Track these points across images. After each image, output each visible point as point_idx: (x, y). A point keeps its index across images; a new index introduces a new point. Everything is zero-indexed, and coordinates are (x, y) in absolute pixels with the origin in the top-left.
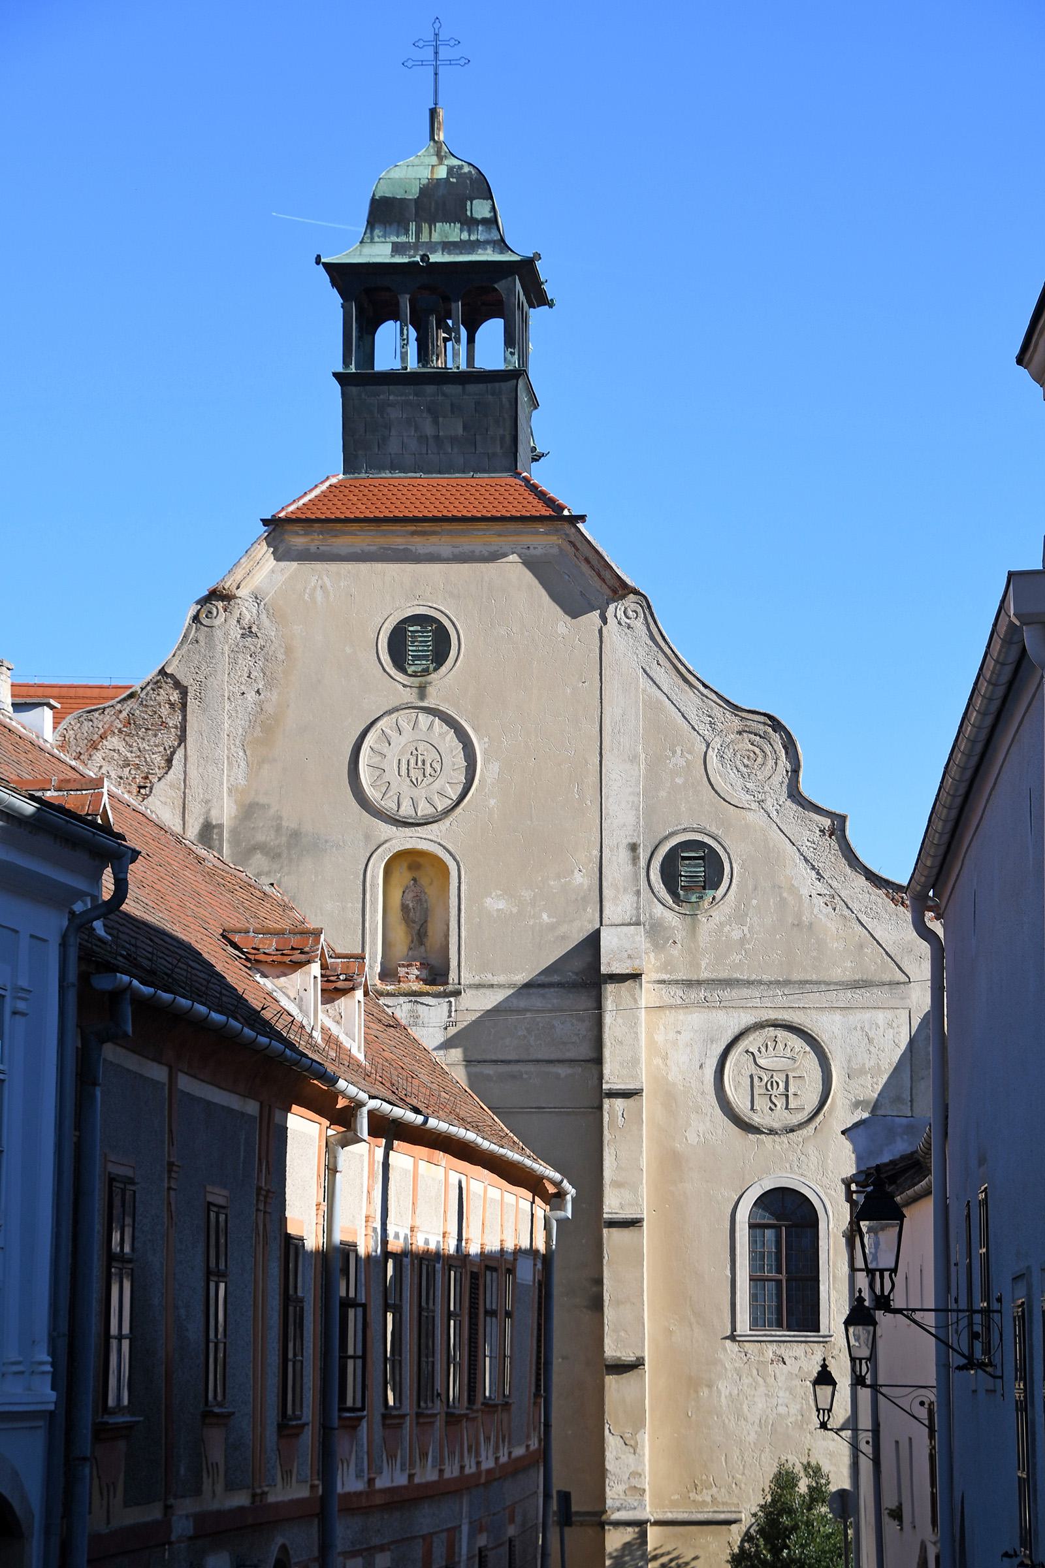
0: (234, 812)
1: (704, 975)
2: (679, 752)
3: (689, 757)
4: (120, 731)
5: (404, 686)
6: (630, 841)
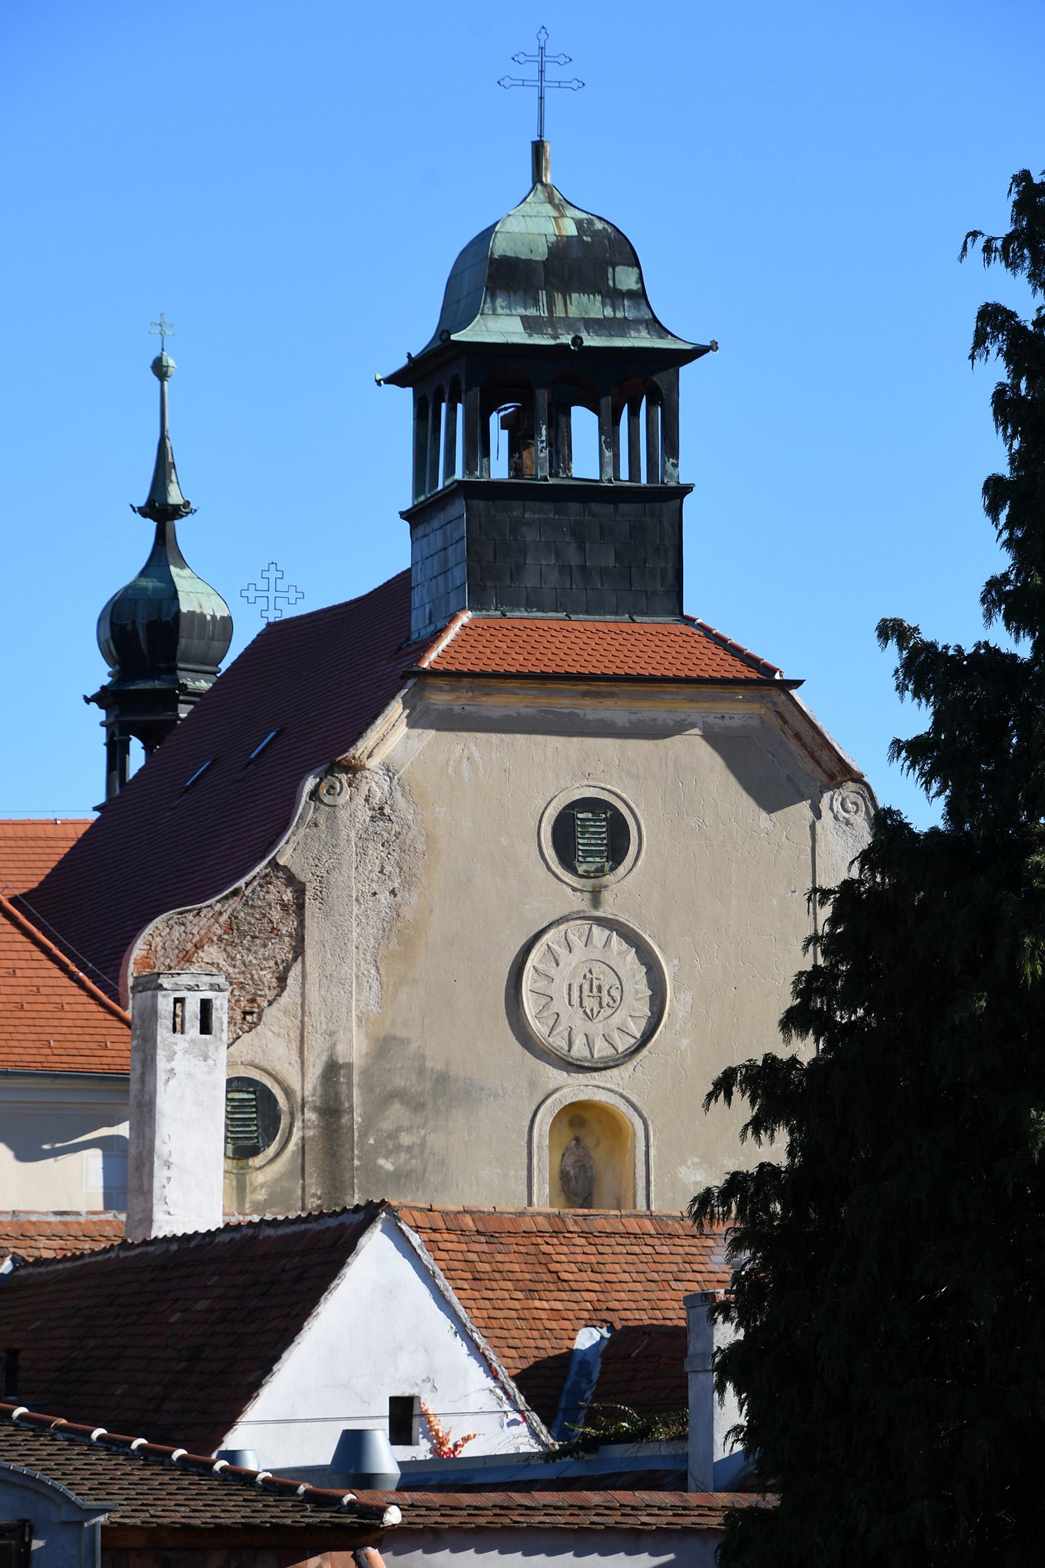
0: (365, 1048)
4: (220, 939)
5: (574, 889)
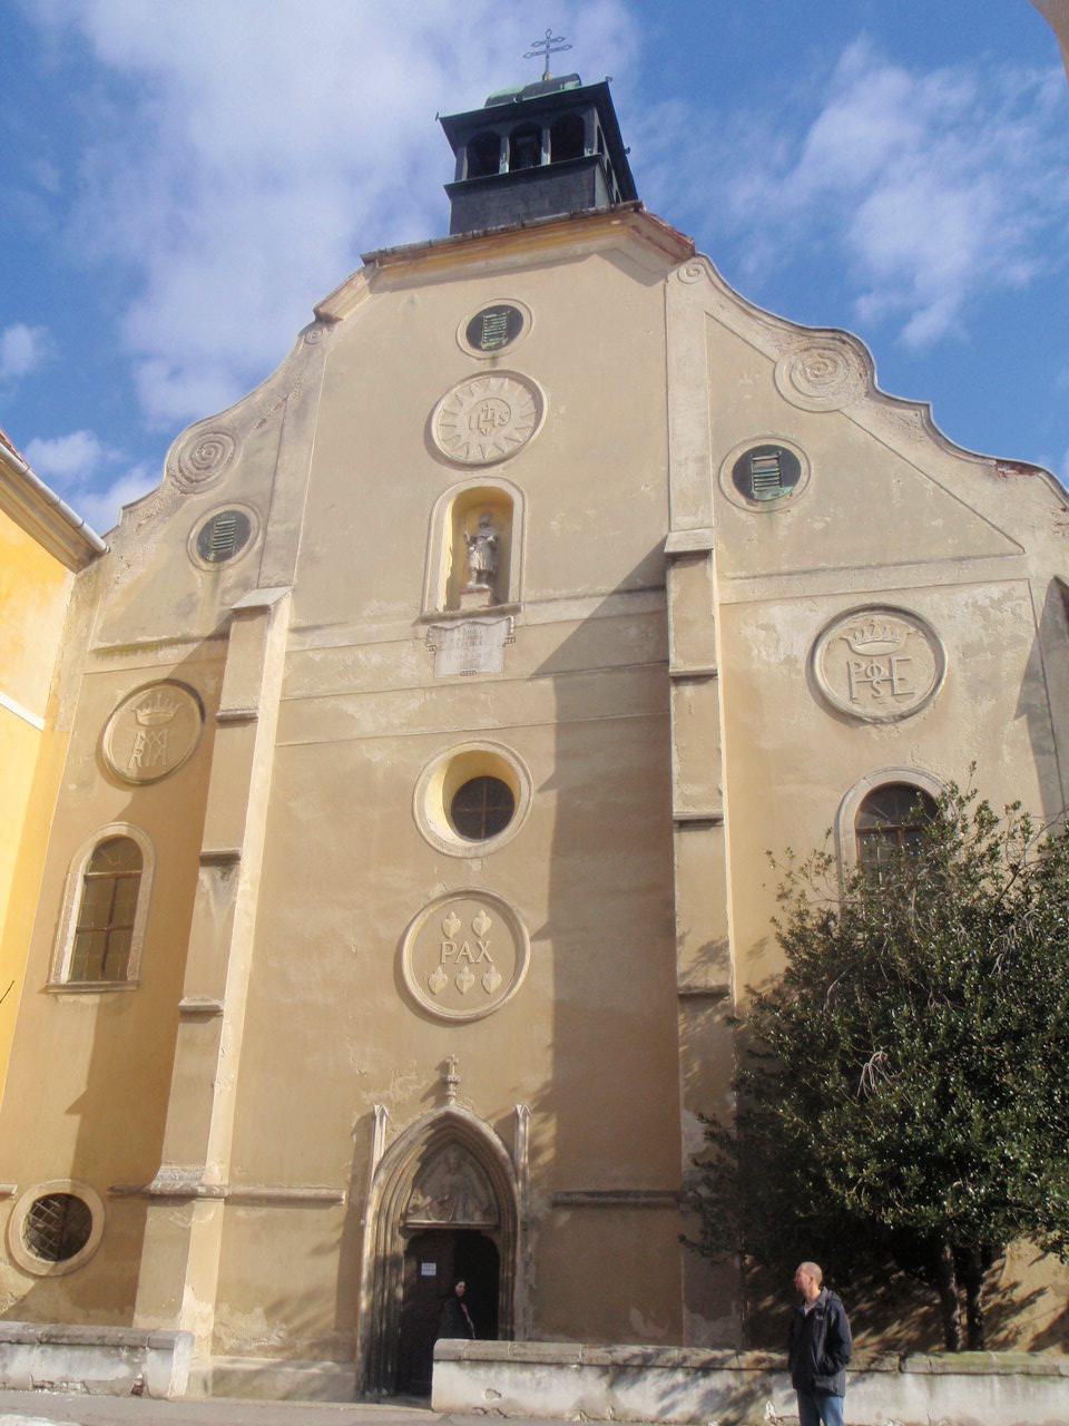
5: (479, 359)
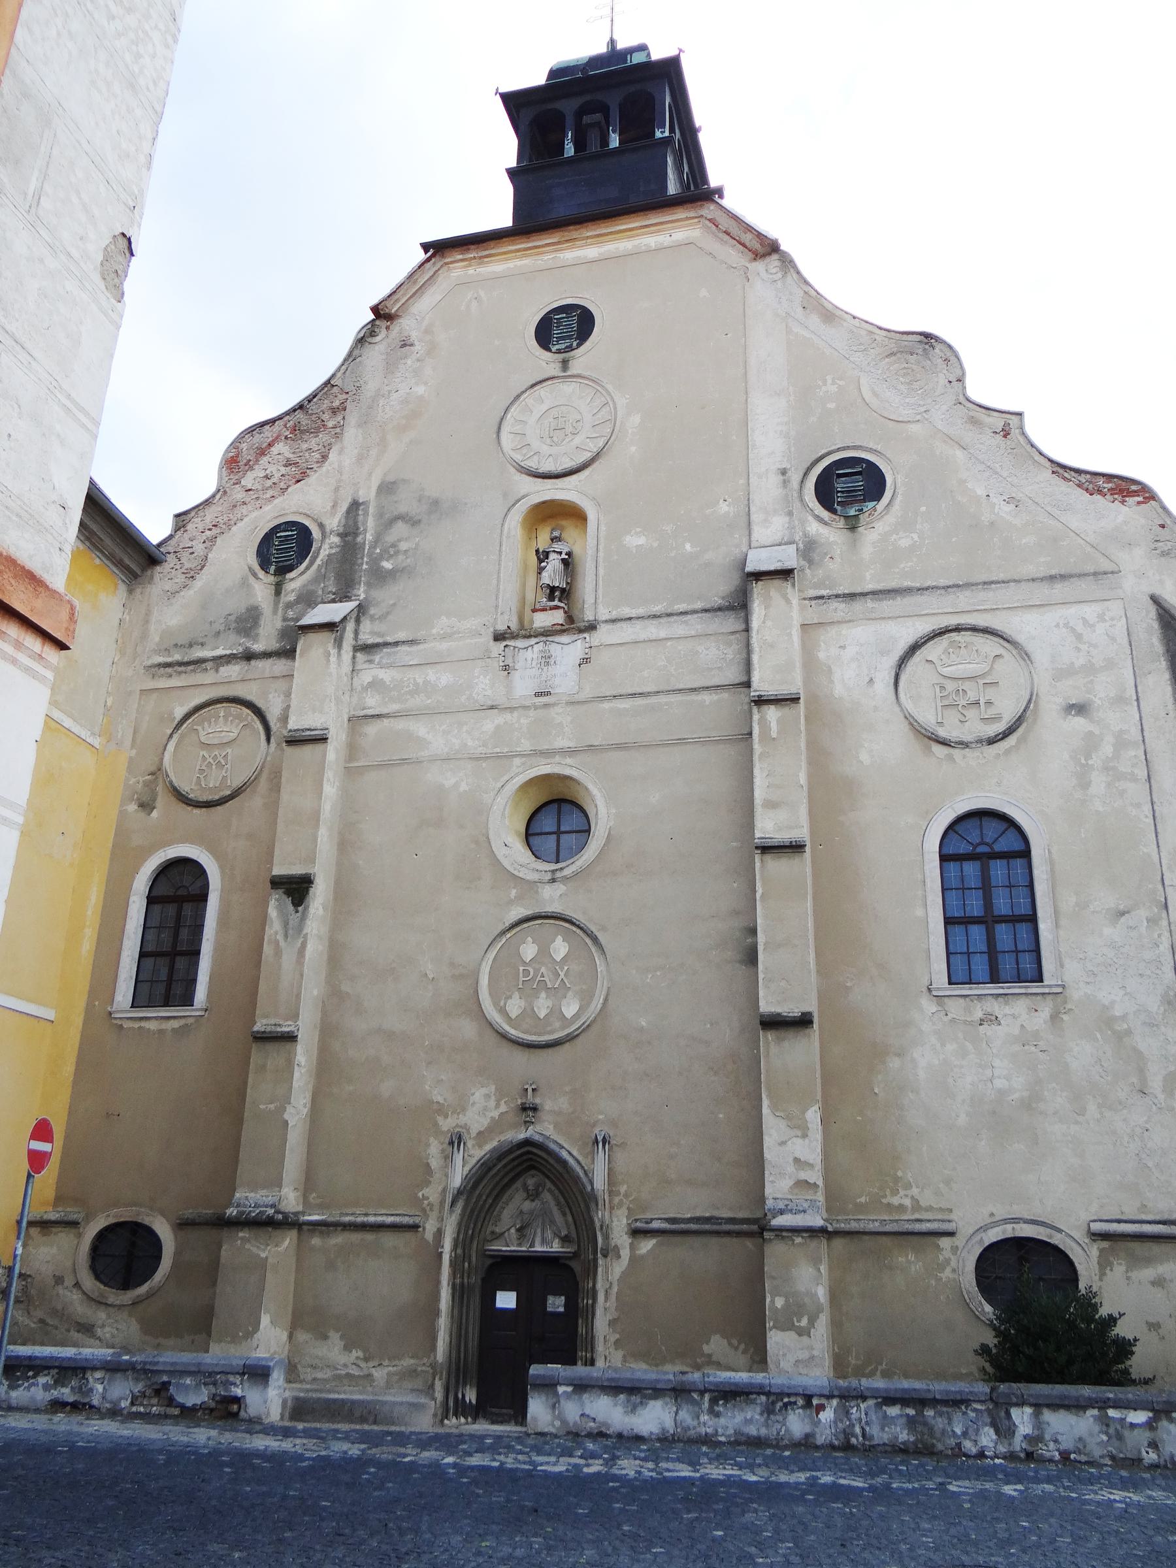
1: (870, 587)
2: (829, 381)
3: (841, 383)
4: (286, 438)
6: (780, 467)
